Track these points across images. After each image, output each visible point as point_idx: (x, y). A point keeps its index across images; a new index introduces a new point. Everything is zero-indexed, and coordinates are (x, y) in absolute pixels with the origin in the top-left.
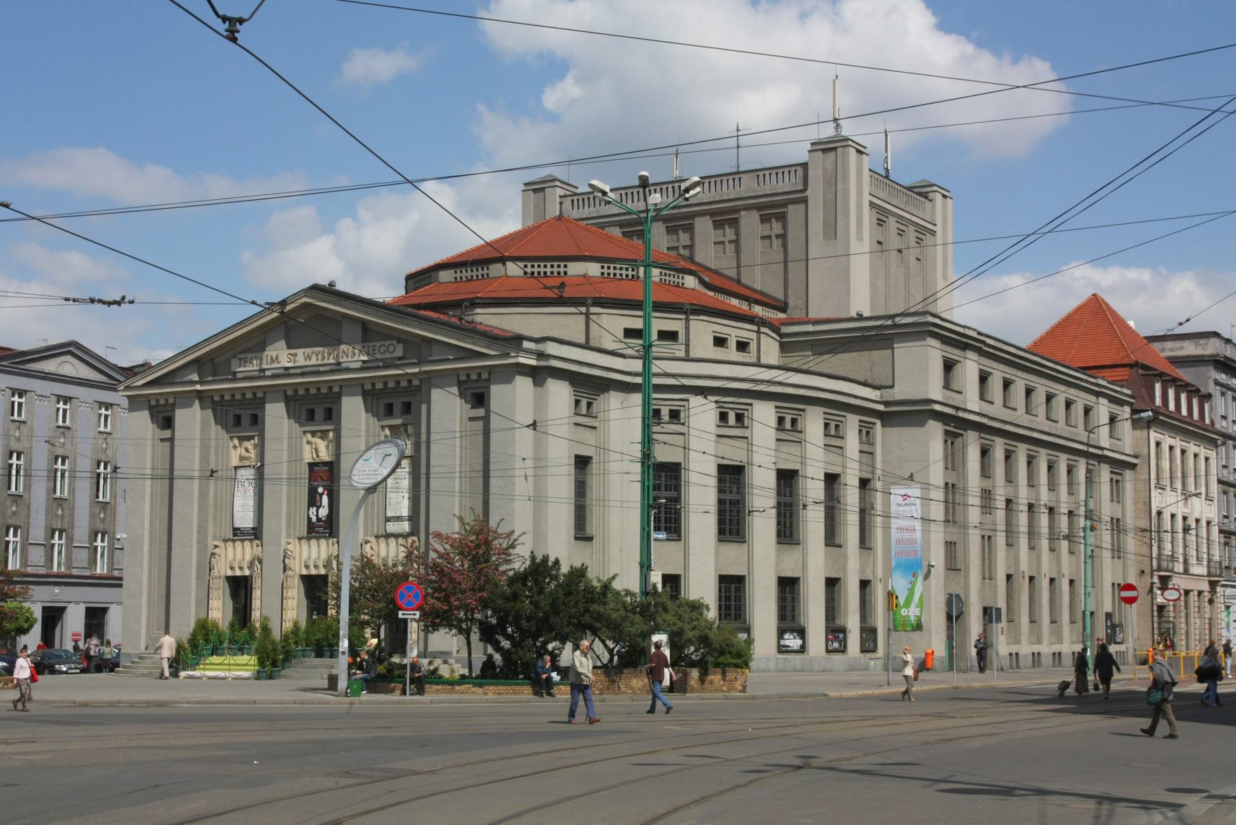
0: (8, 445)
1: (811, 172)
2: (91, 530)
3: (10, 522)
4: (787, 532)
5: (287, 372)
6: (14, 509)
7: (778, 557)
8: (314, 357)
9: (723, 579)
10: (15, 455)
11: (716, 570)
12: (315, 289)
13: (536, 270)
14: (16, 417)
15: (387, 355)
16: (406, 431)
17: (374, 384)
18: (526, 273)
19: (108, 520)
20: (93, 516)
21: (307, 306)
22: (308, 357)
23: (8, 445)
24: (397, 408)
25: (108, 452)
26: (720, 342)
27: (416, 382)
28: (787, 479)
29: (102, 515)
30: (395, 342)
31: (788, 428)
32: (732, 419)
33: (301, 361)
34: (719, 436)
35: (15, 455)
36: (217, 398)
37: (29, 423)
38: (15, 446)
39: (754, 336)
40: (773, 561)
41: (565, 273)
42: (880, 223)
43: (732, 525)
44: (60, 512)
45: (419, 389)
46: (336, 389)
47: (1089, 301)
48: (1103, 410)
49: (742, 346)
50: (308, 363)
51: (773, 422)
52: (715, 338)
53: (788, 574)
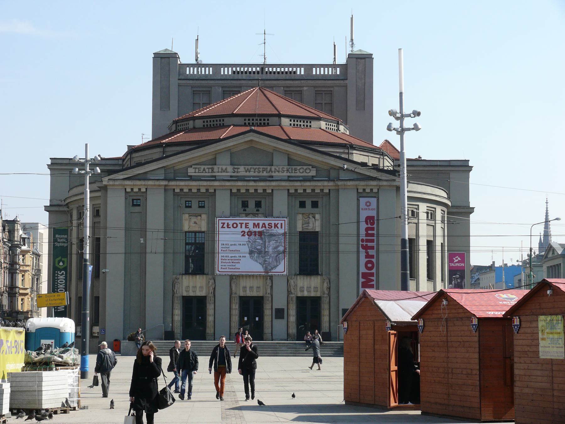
1: (349, 70)
5: (232, 179)
8: (252, 170)
13: (296, 123)
15: (304, 174)
16: (314, 217)
18: (291, 124)
24: (308, 204)
30: (310, 167)
33: (242, 171)
41: (310, 126)
50: (248, 174)
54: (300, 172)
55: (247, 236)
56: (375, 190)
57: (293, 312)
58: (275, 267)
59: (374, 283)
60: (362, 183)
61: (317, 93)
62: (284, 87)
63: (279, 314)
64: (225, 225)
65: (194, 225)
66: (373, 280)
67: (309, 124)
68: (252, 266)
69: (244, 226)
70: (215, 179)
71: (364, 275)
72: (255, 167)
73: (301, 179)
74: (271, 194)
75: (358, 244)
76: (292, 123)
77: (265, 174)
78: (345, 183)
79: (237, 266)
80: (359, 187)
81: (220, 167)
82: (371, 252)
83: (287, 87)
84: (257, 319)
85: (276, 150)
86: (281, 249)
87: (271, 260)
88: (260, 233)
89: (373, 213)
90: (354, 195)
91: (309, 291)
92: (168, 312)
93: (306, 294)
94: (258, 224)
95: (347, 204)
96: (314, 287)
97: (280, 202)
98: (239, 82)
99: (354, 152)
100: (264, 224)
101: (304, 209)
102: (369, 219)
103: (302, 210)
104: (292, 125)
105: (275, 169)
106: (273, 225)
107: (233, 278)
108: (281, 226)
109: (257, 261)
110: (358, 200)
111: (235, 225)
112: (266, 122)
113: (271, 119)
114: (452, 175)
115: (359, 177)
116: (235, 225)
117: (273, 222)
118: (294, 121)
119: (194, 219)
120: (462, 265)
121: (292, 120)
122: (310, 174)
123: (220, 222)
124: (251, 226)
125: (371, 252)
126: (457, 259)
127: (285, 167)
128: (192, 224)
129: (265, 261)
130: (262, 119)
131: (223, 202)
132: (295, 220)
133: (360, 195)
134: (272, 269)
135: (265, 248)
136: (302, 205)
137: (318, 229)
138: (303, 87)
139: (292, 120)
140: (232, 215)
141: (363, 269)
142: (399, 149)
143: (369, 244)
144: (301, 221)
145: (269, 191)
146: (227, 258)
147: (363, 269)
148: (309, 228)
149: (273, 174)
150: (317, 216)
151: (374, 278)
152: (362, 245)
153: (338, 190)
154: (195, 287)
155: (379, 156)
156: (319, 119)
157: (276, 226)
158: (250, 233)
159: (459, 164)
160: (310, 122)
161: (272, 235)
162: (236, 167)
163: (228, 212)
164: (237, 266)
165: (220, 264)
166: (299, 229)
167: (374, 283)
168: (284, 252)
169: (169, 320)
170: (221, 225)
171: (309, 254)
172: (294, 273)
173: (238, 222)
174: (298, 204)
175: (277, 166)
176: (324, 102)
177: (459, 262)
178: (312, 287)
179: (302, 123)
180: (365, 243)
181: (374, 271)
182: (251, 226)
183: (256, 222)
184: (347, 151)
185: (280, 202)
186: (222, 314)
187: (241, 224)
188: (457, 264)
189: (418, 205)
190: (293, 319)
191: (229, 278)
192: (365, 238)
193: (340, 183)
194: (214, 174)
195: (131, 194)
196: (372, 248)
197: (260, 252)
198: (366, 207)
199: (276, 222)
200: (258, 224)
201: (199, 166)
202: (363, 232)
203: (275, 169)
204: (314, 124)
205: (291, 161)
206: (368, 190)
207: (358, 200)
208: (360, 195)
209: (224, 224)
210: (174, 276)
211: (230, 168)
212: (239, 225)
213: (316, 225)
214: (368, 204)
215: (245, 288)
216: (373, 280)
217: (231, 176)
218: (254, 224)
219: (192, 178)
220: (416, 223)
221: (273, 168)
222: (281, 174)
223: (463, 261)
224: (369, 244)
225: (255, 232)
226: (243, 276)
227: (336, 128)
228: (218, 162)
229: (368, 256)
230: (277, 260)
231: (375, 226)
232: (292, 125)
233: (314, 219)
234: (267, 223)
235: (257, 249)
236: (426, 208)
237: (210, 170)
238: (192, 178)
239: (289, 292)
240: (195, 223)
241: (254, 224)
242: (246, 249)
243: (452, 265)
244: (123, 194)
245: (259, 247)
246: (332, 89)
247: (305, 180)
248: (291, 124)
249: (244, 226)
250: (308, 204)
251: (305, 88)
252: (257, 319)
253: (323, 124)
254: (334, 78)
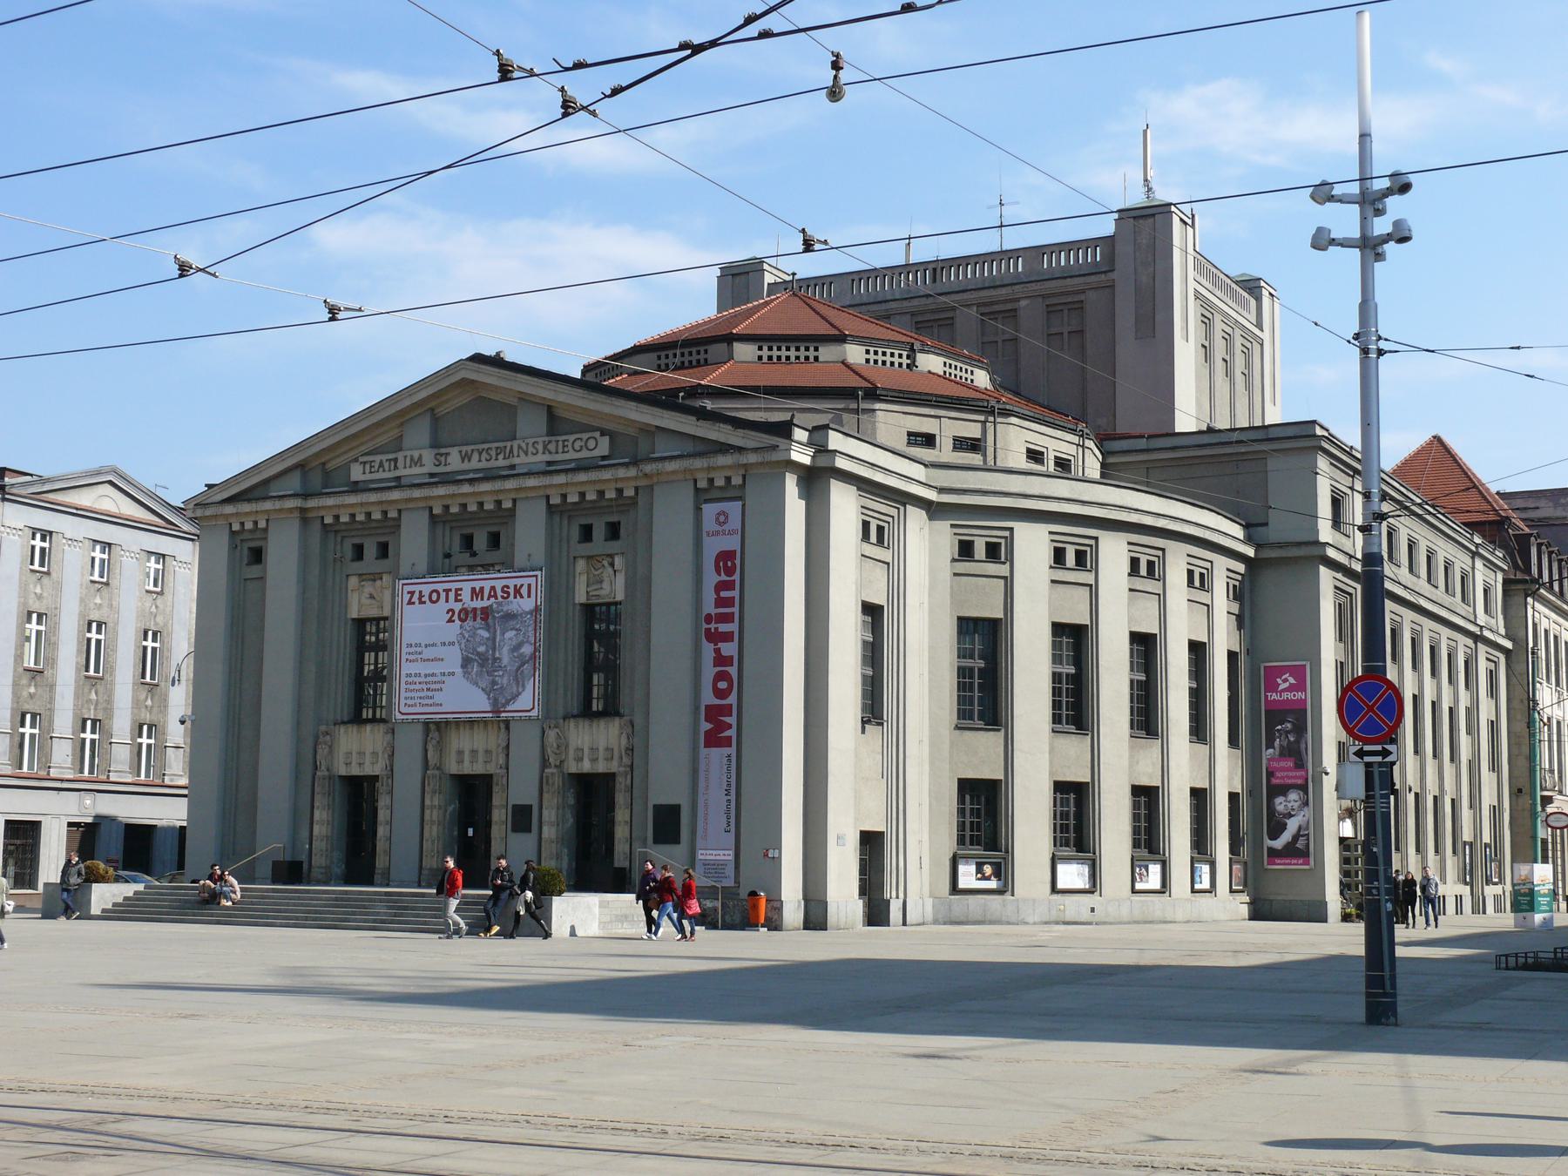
0: (25, 604)
1: (1118, 248)
2: (134, 721)
3: (26, 707)
4: (1146, 719)
6: (32, 690)
7: (1131, 757)
8: (476, 456)
9: (1060, 787)
10: (34, 616)
11: (1051, 774)
12: (478, 358)
14: (36, 567)
15: (584, 454)
16: (612, 565)
17: (564, 496)
18: (760, 358)
19: (155, 710)
20: (137, 704)
21: (465, 383)
22: (466, 457)
23: (25, 604)
24: (599, 532)
25: (160, 619)
26: (1035, 456)
27: (629, 492)
28: (1145, 646)
29: (149, 702)
30: (597, 434)
31: (1146, 570)
32: (1070, 559)
33: (454, 462)
34: (1053, 581)
35: (34, 616)
36: (329, 520)
37: (54, 575)
38: (36, 606)
39: (1072, 450)
40: (1126, 762)
41: (816, 359)
42: (1207, 322)
43: (1074, 706)
44: (93, 696)
45: (633, 501)
46: (507, 505)
47: (1430, 443)
48: (1481, 575)
49: (1063, 464)
50: (466, 466)
51: (1126, 568)
52: (1029, 451)
53: (1145, 781)
54: (574, 449)
55: (458, 622)
56: (737, 481)
58: (515, 697)
59: (732, 733)
60: (698, 463)
61: (1051, 311)
62: (978, 305)
63: (522, 818)
64: (415, 598)
65: (369, 601)
66: (730, 726)
67: (811, 354)
68: (463, 697)
69: (452, 595)
70: (398, 483)
71: (714, 713)
73: (573, 465)
75: (697, 626)
76: (765, 353)
77: (501, 462)
78: (660, 465)
79: (438, 697)
80: (699, 476)
81: (408, 453)
82: (728, 649)
83: (985, 305)
84: (470, 832)
85: (524, 398)
86: (527, 650)
87: (505, 681)
88: (486, 613)
89: (732, 543)
90: (686, 496)
91: (594, 760)
92: (301, 816)
93: (586, 767)
94: (482, 589)
95: (670, 518)
96: (607, 749)
97: (529, 534)
98: (884, 306)
99: (878, 406)
100: (493, 588)
101: (588, 545)
102: (725, 557)
103: (586, 549)
104: (765, 359)
105: (520, 447)
106: (512, 591)
107: (437, 729)
108: (525, 592)
109: (476, 684)
110: (698, 509)
111: (434, 597)
112: (702, 357)
113: (713, 348)
114: (1273, 463)
115: (701, 448)
116: (434, 597)
117: (511, 583)
118: (770, 349)
119: (368, 588)
120: (1300, 695)
121: (765, 348)
122: (596, 453)
123: (407, 589)
124: (466, 595)
125: (728, 649)
126: (1285, 681)
127: (540, 440)
128: (365, 601)
129: (494, 683)
130: (694, 350)
131: (414, 542)
132: (571, 575)
133: (702, 496)
134: (508, 702)
135: (494, 649)
136: (587, 534)
137: (620, 597)
138: (1018, 300)
139: (765, 348)
140: (433, 571)
141: (708, 698)
142: (1351, 436)
143: (723, 628)
144: (584, 578)
145: (507, 505)
146: (417, 680)
147: (708, 698)
148: (602, 592)
149: (516, 461)
150: (618, 561)
151: (732, 720)
152: (708, 630)
153: (651, 488)
155: (982, 418)
156: (841, 339)
157: (517, 591)
158: (465, 614)
159: (1290, 432)
160: (816, 349)
161: (510, 616)
162: (443, 451)
163: (422, 566)
164: (438, 697)
165: (403, 694)
166: (581, 597)
167: (732, 733)
168: (533, 657)
169: (305, 834)
170: (407, 597)
171: (597, 662)
172: (561, 712)
173: (440, 587)
174: (575, 533)
175: (524, 439)
176: (1065, 330)
177: (1291, 689)
179: (792, 353)
180: (713, 626)
181: (732, 699)
182: (466, 595)
183: (477, 585)
184: (853, 406)
185: (529, 534)
186: (410, 821)
187: (447, 591)
188: (1286, 696)
189: (1011, 529)
191: (420, 727)
192: (713, 611)
193: (649, 468)
194: (397, 473)
195: (246, 536)
196: (728, 637)
197: (483, 660)
198: (718, 528)
199: (518, 582)
200: (482, 589)
201: (370, 458)
202: (709, 596)
203: (520, 447)
204: (827, 353)
205: (555, 422)
206: (720, 482)
207: (698, 509)
208: (702, 496)
209: (412, 593)
211: (428, 456)
212: (443, 595)
213: (615, 588)
214: (722, 518)
215: (460, 753)
216: (730, 726)
217: (432, 475)
218: (473, 589)
219: (356, 488)
220: (1005, 578)
221: (515, 444)
222: (532, 459)
223: (1300, 686)
224: (723, 628)
225: (475, 610)
226: (458, 723)
227: (905, 361)
228: (406, 443)
229: (721, 660)
230: (518, 679)
231: (736, 577)
232: (765, 359)
233: (610, 570)
234: (499, 585)
235: (478, 654)
236: (1047, 537)
238: (356, 488)
239: (545, 763)
240: (372, 597)
241: (473, 589)
242: (453, 658)
243: (1275, 696)
244: (226, 537)
245: (482, 649)
246: (1082, 297)
247: (582, 466)
248: (760, 358)
249: (452, 595)
250: (599, 532)
251: (1023, 303)
252: (470, 832)
253: (855, 353)
254: (1094, 271)
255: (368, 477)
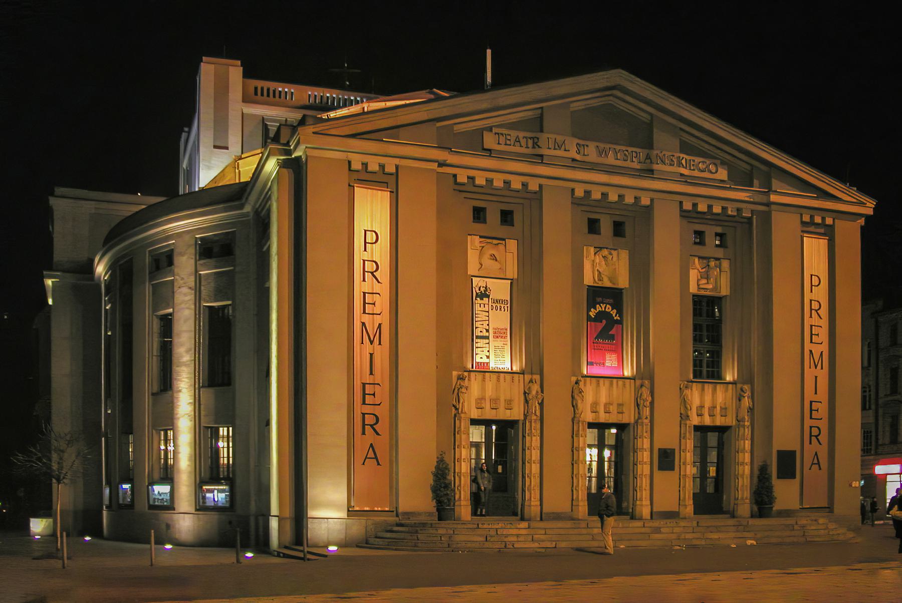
15: (706, 175)
57: (689, 456)
63: (666, 459)
72: (618, 148)
74: (649, 209)
137: (725, 291)
154: (495, 401)
178: (718, 408)
190: (691, 470)
201: (505, 131)
210: (455, 373)
237: (530, 142)
255: (502, 148)
